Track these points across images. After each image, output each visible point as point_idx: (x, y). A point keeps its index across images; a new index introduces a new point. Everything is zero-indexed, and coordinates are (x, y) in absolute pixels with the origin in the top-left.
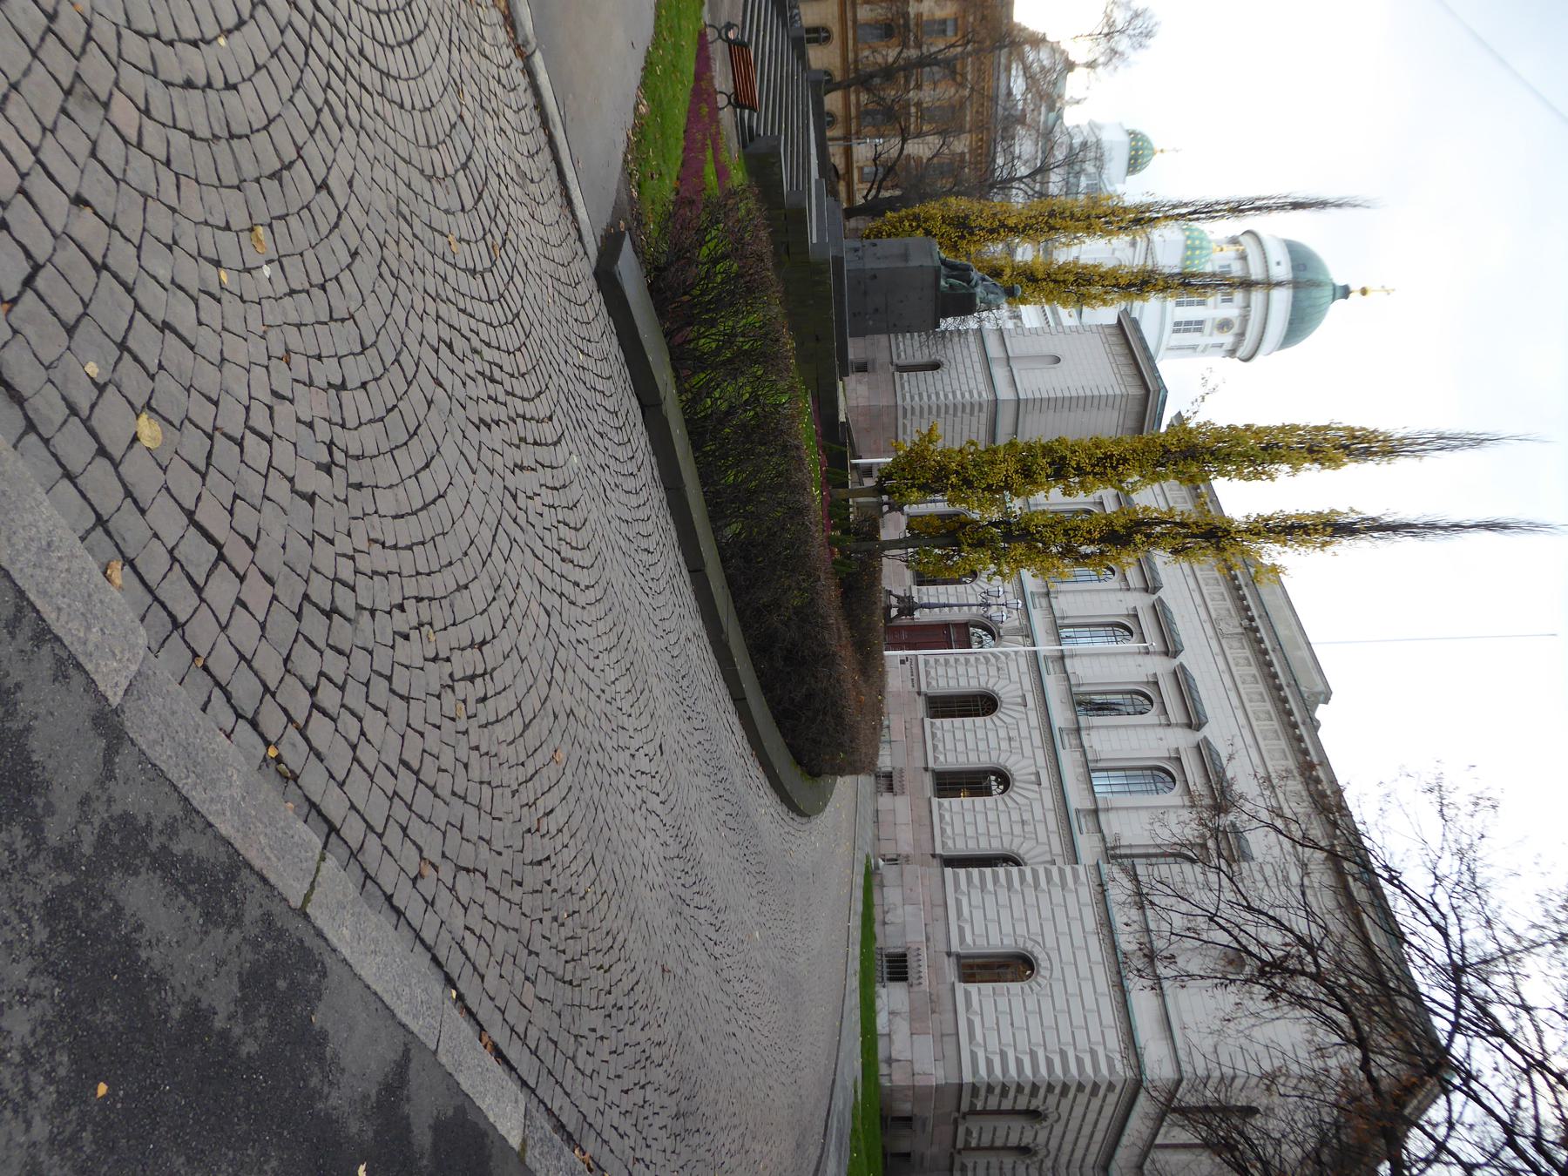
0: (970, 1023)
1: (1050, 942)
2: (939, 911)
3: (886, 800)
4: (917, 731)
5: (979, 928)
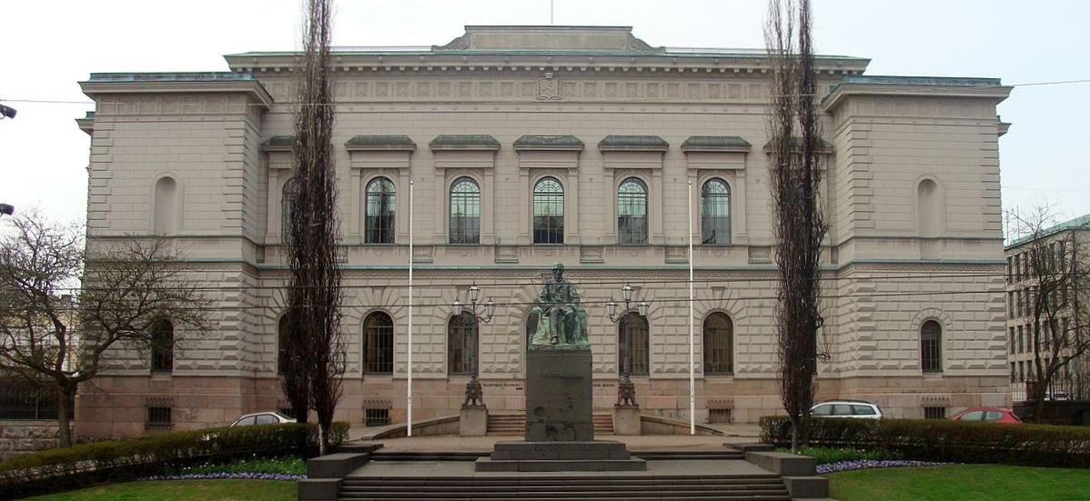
0: (973, 367)
1: (916, 306)
2: (892, 382)
3: (738, 415)
4: (664, 385)
5: (906, 355)
